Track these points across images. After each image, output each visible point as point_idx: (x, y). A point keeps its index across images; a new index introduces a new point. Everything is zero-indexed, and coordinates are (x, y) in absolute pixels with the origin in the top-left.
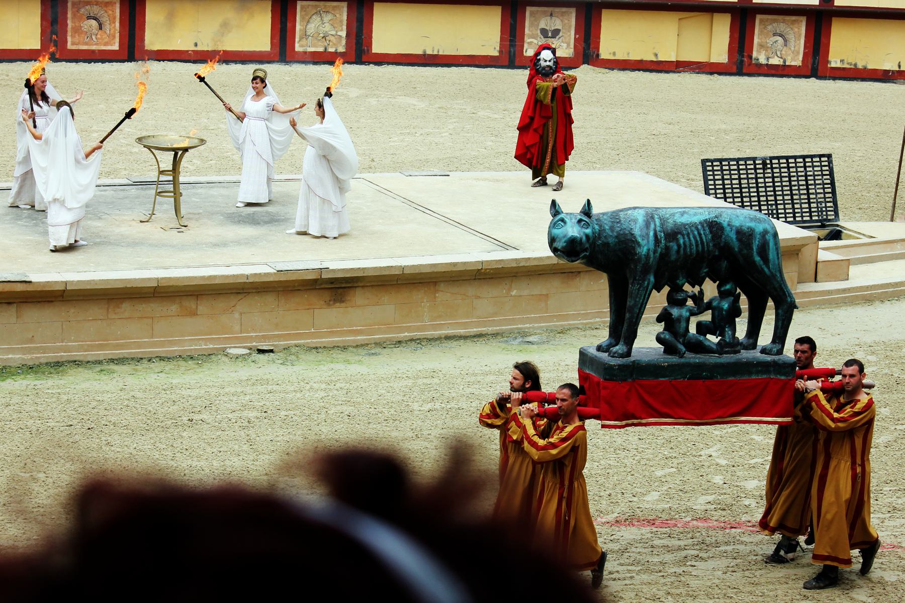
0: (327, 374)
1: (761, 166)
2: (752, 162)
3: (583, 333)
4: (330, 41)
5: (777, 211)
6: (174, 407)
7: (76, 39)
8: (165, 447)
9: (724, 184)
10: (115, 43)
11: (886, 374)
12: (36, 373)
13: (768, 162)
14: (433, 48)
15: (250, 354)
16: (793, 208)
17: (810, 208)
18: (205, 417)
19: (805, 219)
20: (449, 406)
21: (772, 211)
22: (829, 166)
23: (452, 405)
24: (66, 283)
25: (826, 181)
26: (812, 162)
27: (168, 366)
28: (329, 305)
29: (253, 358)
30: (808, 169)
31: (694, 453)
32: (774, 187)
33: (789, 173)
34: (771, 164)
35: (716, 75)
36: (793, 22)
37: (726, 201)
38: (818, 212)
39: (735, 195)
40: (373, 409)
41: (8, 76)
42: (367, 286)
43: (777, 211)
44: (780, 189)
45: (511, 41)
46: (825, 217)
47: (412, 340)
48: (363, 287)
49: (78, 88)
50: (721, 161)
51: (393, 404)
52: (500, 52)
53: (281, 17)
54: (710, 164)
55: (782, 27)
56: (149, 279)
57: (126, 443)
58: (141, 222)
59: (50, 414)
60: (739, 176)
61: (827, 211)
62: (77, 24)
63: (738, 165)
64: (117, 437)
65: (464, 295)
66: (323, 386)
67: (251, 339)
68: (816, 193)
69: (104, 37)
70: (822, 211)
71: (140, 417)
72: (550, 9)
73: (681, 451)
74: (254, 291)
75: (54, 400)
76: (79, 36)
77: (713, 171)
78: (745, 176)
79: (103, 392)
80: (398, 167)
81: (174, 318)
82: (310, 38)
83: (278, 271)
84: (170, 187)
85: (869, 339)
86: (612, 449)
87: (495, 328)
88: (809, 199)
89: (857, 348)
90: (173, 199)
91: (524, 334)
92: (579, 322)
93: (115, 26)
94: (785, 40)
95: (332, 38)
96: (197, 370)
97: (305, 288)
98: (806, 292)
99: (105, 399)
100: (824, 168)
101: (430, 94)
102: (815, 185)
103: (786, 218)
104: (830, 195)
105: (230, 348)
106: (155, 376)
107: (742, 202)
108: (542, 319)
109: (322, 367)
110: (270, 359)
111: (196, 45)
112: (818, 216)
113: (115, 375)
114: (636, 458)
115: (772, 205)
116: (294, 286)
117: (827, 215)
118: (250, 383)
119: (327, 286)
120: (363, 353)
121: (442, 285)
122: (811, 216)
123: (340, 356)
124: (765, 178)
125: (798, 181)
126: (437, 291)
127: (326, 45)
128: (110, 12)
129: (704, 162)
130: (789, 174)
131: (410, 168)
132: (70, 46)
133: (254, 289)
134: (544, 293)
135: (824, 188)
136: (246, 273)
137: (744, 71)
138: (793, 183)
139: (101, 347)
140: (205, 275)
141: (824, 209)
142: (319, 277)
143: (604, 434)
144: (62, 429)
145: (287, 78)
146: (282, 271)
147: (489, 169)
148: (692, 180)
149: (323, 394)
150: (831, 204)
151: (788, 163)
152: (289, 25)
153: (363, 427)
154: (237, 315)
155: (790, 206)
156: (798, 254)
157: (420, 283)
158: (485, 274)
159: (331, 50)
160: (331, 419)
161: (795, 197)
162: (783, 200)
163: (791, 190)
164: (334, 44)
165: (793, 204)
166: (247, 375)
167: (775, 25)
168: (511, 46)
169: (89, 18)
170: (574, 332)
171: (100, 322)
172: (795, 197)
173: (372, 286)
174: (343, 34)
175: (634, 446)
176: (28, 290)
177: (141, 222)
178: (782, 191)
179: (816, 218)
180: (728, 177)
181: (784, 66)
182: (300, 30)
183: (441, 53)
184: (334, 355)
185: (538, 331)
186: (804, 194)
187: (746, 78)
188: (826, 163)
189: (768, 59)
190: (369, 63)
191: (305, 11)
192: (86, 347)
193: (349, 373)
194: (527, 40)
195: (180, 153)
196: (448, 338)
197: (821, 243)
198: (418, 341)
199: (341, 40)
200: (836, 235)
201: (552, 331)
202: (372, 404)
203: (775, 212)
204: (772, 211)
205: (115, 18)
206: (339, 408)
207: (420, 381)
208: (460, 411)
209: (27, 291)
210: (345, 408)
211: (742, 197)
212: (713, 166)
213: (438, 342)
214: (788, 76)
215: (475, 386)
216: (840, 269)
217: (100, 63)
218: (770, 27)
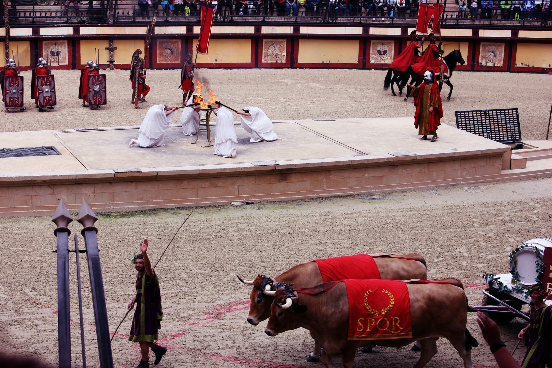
0: (278, 214)
1: (484, 114)
2: (479, 113)
3: (399, 194)
5: (492, 136)
6: (208, 230)
7: (161, 59)
8: (204, 248)
9: (466, 123)
11: (545, 213)
12: (144, 214)
13: (487, 112)
15: (243, 205)
16: (499, 134)
17: (507, 134)
18: (222, 234)
19: (505, 139)
20: (336, 229)
21: (489, 136)
22: (516, 114)
23: (338, 228)
24: (157, 172)
25: (515, 121)
26: (508, 112)
27: (205, 211)
29: (244, 207)
30: (506, 116)
31: (453, 251)
32: (490, 124)
33: (497, 117)
34: (489, 113)
35: (461, 71)
36: (499, 46)
37: (467, 131)
38: (511, 136)
39: (471, 128)
40: (300, 230)
43: (492, 136)
44: (493, 125)
45: (364, 56)
46: (514, 138)
47: (318, 198)
48: (295, 173)
50: (464, 112)
51: (310, 228)
52: (359, 61)
54: (459, 113)
55: (493, 48)
56: (196, 170)
57: (186, 247)
58: (192, 143)
59: (151, 233)
60: (473, 119)
61: (515, 135)
63: (473, 114)
64: (181, 244)
66: (277, 220)
67: (243, 198)
68: (510, 127)
70: (513, 136)
71: (192, 235)
72: (382, 41)
73: (446, 250)
75: (152, 226)
77: (461, 117)
78: (476, 119)
79: (175, 223)
80: (311, 116)
81: (207, 188)
84: (205, 127)
85: (536, 196)
86: (414, 249)
87: (357, 192)
88: (507, 130)
89: (530, 201)
90: (206, 133)
91: (371, 195)
92: (397, 189)
94: (495, 55)
95: (279, 56)
96: (218, 212)
98: (506, 174)
99: (176, 226)
100: (514, 115)
102: (510, 123)
103: (496, 139)
104: (517, 128)
105: (233, 202)
106: (199, 215)
107: (475, 131)
108: (379, 188)
109: (276, 210)
110: (252, 207)
111: (216, 60)
112: (511, 138)
113: (180, 215)
114: (425, 253)
115: (489, 133)
117: (515, 137)
118: (243, 218)
120: (295, 204)
121: (332, 172)
122: (508, 138)
123: (285, 205)
124: (485, 120)
125: (502, 121)
128: (177, 46)
129: (456, 113)
130: (497, 118)
131: (317, 117)
132: (158, 62)
134: (381, 175)
135: (514, 125)
137: (475, 69)
138: (499, 122)
139: (174, 202)
141: (514, 135)
143: (409, 242)
144: (156, 240)
145: (258, 75)
147: (354, 117)
148: (451, 121)
149: (277, 223)
150: (518, 132)
151: (497, 113)
152: (259, 50)
153: (296, 239)
154: (236, 187)
155: (498, 133)
156: (502, 156)
158: (353, 166)
159: (279, 62)
160: (281, 235)
161: (500, 129)
162: (495, 130)
163: (498, 126)
165: (499, 132)
166: (241, 214)
167: (490, 47)
168: (364, 59)
169: (167, 49)
170: (395, 194)
171: (173, 190)
172: (500, 129)
173: (300, 172)
174: (285, 54)
175: (424, 248)
176: (140, 175)
177: (192, 143)
178: (494, 126)
179: (511, 139)
180: (468, 120)
181: (494, 67)
182: (265, 53)
184: (282, 205)
185: (378, 193)
186: (505, 128)
187: (476, 72)
188: (515, 113)
189: (486, 63)
192: (167, 202)
193: (289, 213)
194: (371, 56)
195: (210, 111)
196: (336, 197)
197: (513, 150)
198: (321, 198)
200: (520, 147)
201: (384, 193)
202: (300, 228)
203: (490, 136)
204: (489, 136)
206: (284, 230)
207: (322, 217)
208: (341, 231)
210: (287, 230)
211: (475, 129)
212: (460, 114)
213: (331, 199)
214: (496, 71)
215: (348, 219)
216: (522, 163)
218: (487, 48)
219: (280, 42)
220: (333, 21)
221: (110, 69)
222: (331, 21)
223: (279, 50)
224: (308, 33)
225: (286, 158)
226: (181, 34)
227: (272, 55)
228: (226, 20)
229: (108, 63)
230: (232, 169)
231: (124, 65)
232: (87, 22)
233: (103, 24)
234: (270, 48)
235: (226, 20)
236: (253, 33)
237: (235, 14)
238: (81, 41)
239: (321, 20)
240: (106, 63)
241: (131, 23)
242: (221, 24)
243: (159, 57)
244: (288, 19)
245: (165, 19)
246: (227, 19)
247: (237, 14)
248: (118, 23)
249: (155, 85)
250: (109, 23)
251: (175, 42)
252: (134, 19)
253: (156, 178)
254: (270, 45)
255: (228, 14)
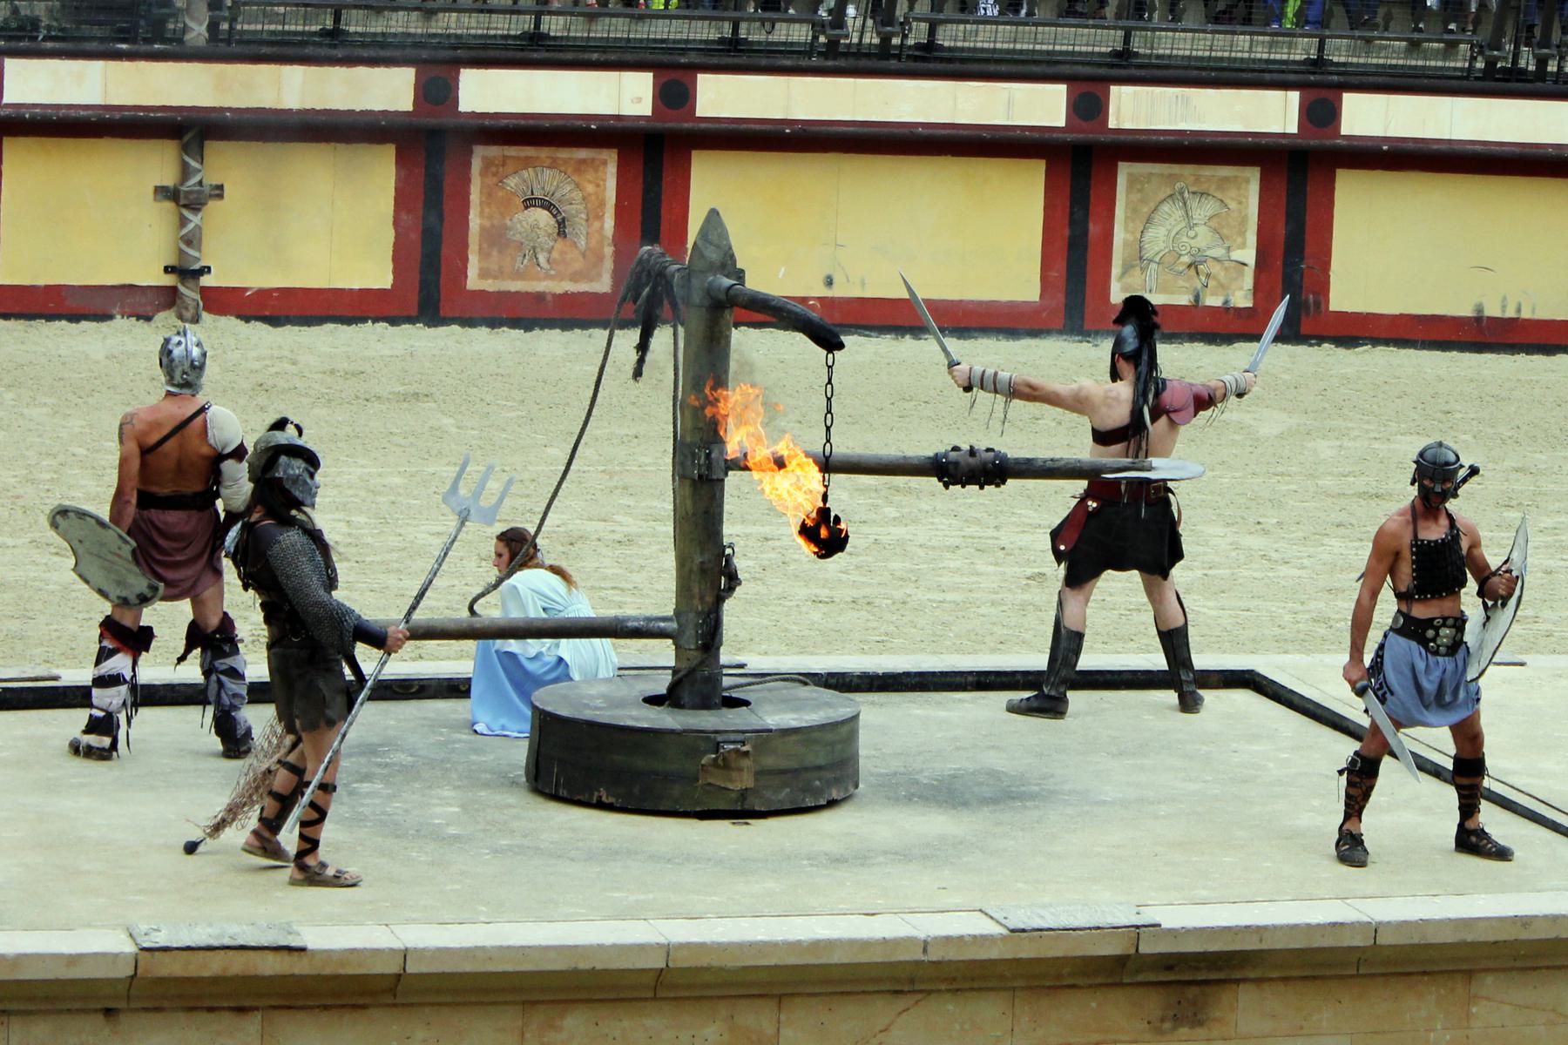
4: (1208, 276)
10: (600, 275)
14: (1505, 299)
28: (1159, 1032)
41: (294, 363)
42: (1271, 979)
48: (1259, 981)
49: (488, 398)
53: (1072, 207)
56: (642, 948)
62: (496, 222)
65: (1554, 1010)
69: (568, 257)
74: (943, 987)
76: (500, 252)
82: (1153, 266)
83: (1013, 931)
93: (602, 228)
95: (1215, 269)
97: (1090, 982)
101: (1490, 431)
111: (829, 282)
116: (1059, 976)
119: (1153, 977)
121: (1489, 979)
126: (1473, 999)
127: (1199, 286)
128: (590, 188)
132: (473, 282)
133: (945, 980)
136: (922, 936)
140: (802, 938)
142: (1132, 951)
146: (1023, 931)
152: (1094, 229)
157: (1424, 973)
159: (1213, 301)
164: (1222, 286)
169: (529, 203)
173: (1285, 979)
174: (1249, 255)
176: (297, 971)
182: (1126, 244)
183: (1526, 314)
190: (1321, 339)
191: (1139, 191)
199: (1241, 274)
205: (602, 204)
209: (293, 976)
217: (558, 331)
219: (1223, 183)
220: (1542, 62)
221: (181, 317)
222: (1532, 68)
223: (1216, 231)
224: (1389, 134)
225: (1203, 893)
226: (618, 117)
227: (1167, 262)
228: (896, 41)
229: (169, 280)
230: (865, 944)
231: (264, 294)
232: (49, 28)
233: (147, 41)
234: (1157, 218)
235: (896, 41)
236: (1061, 123)
237: (949, 10)
238: (7, 141)
239: (1473, 59)
240: (153, 276)
241: (320, 45)
242: (864, 63)
243: (484, 255)
244: (1271, 45)
245: (520, 25)
246: (905, 37)
247: (963, 10)
248: (240, 42)
249: (447, 421)
250: (180, 41)
251: (581, 165)
252: (337, 19)
253: (392, 991)
254: (1162, 196)
255: (911, 8)
